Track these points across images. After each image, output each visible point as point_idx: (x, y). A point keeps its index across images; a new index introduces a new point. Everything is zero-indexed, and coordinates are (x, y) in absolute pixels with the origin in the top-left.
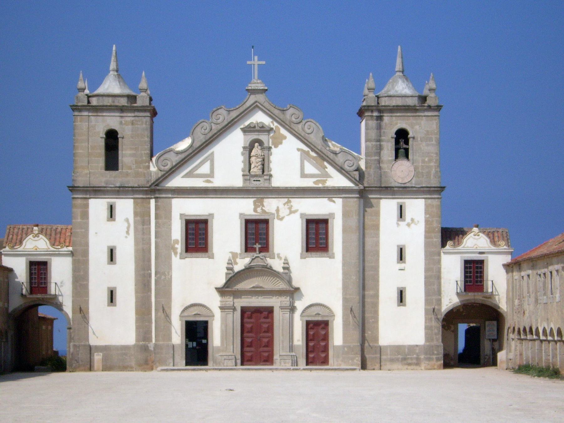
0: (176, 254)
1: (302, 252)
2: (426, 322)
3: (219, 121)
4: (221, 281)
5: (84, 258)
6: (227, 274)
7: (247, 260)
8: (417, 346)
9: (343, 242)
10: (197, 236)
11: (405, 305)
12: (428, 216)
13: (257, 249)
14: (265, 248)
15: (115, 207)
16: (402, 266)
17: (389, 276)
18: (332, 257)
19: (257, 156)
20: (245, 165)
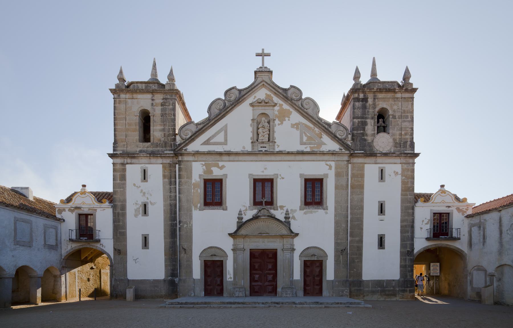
0: (196, 207)
3: (231, 99)
4: (233, 229)
6: (238, 222)
7: (255, 212)
8: (394, 280)
10: (213, 193)
11: (384, 248)
12: (404, 178)
14: (271, 203)
16: (382, 217)
17: (372, 226)
19: (263, 127)
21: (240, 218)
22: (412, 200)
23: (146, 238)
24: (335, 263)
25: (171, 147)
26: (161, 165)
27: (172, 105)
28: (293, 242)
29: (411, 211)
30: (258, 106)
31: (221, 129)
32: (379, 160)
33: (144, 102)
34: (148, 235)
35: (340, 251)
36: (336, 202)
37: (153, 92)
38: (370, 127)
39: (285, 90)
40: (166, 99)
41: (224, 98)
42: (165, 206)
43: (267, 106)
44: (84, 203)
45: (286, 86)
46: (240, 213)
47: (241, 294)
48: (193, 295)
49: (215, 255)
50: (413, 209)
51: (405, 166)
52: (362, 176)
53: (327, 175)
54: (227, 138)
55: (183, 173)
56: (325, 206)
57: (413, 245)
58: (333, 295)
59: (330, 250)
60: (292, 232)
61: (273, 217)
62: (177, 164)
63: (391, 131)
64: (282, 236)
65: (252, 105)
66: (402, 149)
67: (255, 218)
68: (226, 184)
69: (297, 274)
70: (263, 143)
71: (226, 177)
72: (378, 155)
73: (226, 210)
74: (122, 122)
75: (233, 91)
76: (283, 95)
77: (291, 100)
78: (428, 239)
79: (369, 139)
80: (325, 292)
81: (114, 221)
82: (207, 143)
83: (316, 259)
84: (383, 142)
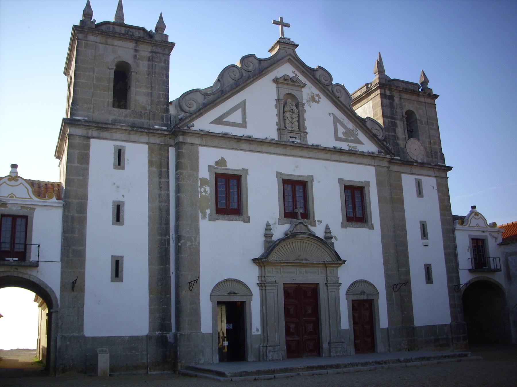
1: (343, 220)
2: (450, 301)
3: (249, 68)
4: (258, 251)
5: (81, 215)
7: (286, 227)
8: (445, 325)
9: (380, 213)
10: (229, 196)
13: (299, 215)
14: (306, 215)
15: (124, 153)
18: (371, 227)
19: (292, 111)
20: (279, 119)
21: (268, 236)
22: (451, 222)
24: (387, 304)
25: (163, 121)
26: (146, 146)
29: (451, 235)
30: (284, 84)
31: (238, 105)
34: (122, 257)
36: (382, 219)
39: (313, 70)
41: (239, 65)
42: (151, 210)
43: (295, 86)
44: (12, 196)
45: (315, 67)
46: (268, 228)
47: (276, 357)
49: (234, 293)
51: (440, 180)
53: (368, 183)
54: (245, 118)
56: (370, 224)
57: (458, 278)
58: (389, 350)
59: (380, 283)
62: (171, 146)
64: (325, 265)
65: (276, 81)
66: (434, 160)
67: (289, 236)
68: (246, 184)
69: (345, 322)
70: (293, 132)
71: (247, 173)
72: (415, 164)
73: (248, 221)
74: (87, 74)
75: (251, 59)
80: (381, 347)
81: (65, 231)
82: (219, 121)
83: (365, 298)
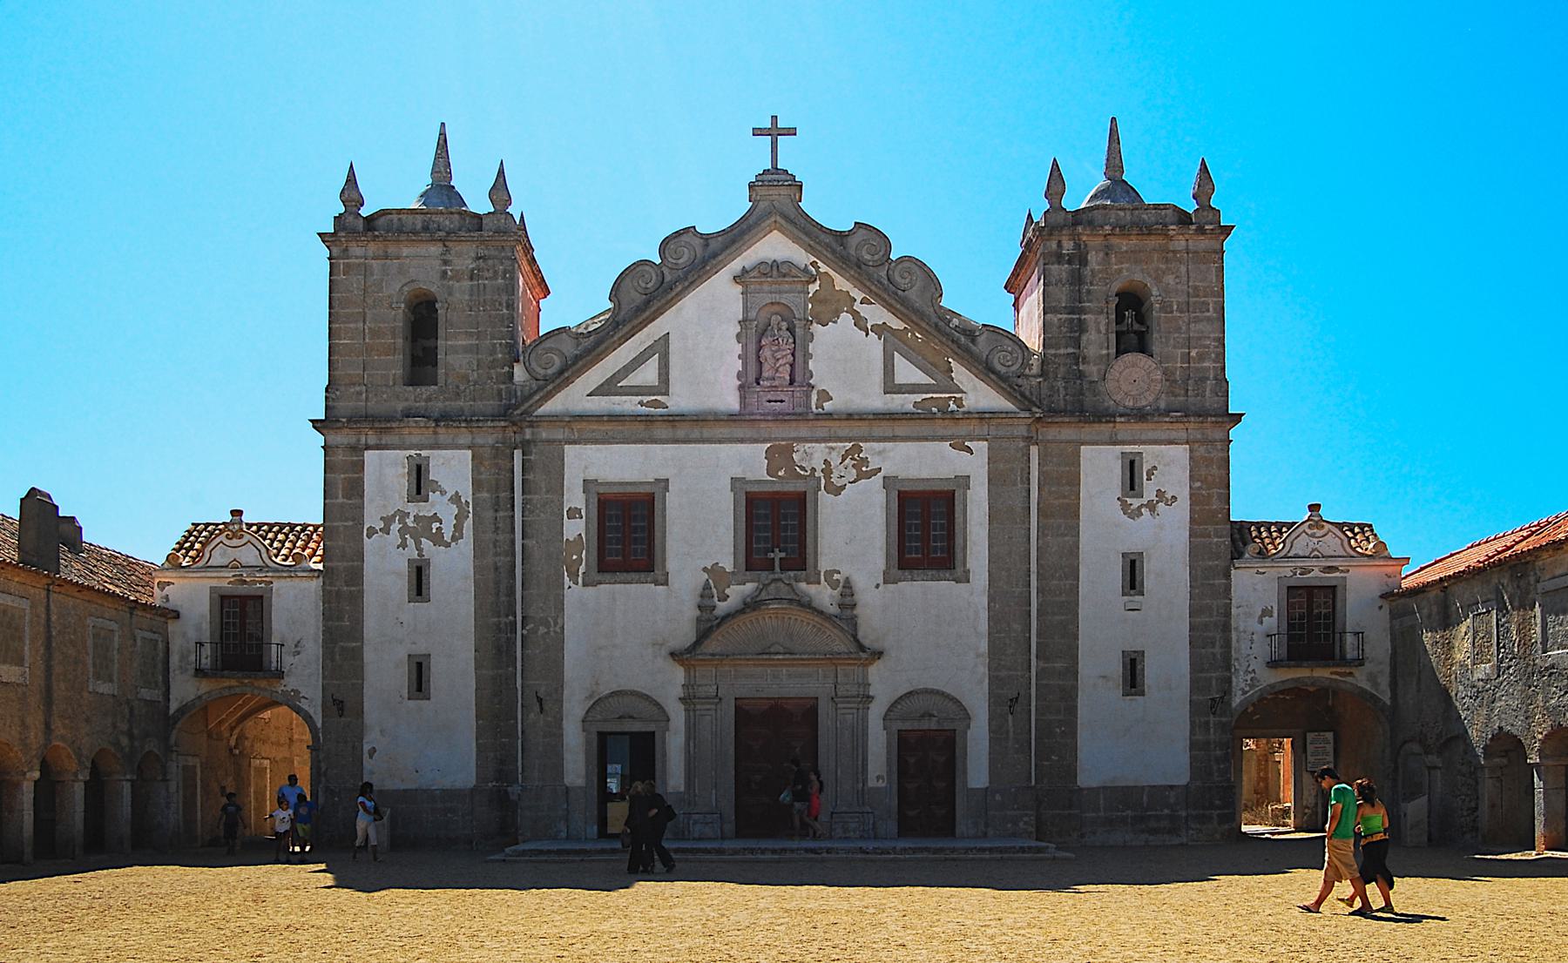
12: (1198, 484)
14: (799, 558)
21: (705, 606)
23: (420, 665)
27: (504, 278)
28: (865, 676)
32: (1124, 429)
33: (421, 265)
35: (1006, 702)
37: (447, 238)
38: (1098, 336)
39: (840, 236)
40: (483, 258)
41: (658, 261)
48: (564, 835)
50: (1228, 576)
51: (1201, 451)
52: (1075, 481)
53: (965, 481)
55: (536, 476)
56: (959, 570)
60: (862, 648)
61: (807, 605)
63: (1156, 349)
67: (751, 605)
75: (684, 238)
76: (834, 252)
77: (859, 264)
78: (1273, 664)
79: (1092, 370)
83: (934, 726)
84: (1133, 379)
